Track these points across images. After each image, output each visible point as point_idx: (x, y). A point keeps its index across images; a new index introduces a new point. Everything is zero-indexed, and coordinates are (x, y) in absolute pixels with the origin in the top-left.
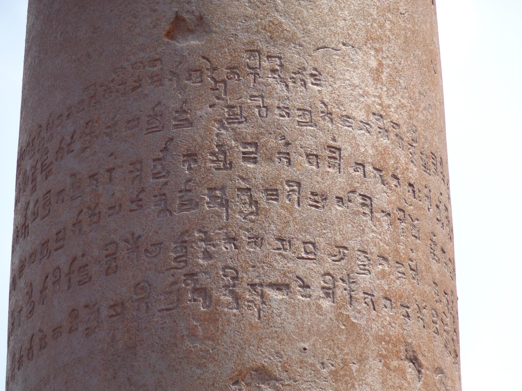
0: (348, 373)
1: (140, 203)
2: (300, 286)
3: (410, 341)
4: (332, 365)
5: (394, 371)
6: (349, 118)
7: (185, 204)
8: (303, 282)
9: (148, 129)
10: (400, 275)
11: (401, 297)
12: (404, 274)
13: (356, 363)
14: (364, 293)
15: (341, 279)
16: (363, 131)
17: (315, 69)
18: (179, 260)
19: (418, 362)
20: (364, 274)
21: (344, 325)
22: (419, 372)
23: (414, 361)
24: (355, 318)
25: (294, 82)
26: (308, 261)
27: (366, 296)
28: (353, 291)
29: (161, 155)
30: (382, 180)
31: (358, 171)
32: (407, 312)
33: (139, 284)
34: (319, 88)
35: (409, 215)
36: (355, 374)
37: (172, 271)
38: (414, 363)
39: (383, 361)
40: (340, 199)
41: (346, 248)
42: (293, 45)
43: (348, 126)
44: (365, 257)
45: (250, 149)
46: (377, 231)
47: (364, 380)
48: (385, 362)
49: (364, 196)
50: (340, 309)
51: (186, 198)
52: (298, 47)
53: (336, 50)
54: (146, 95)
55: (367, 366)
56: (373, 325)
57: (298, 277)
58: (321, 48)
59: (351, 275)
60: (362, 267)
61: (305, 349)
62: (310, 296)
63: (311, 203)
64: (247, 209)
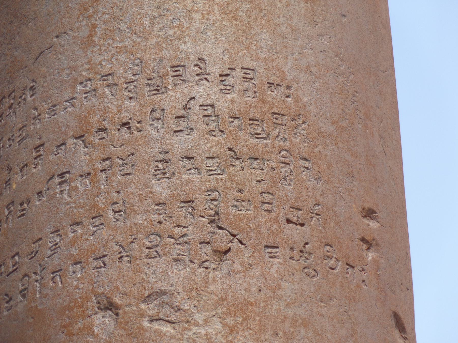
2: (7, 302)
3: (100, 291)
5: (78, 334)
11: (93, 252)
12: (102, 224)
14: (53, 273)
17: (33, 81)
19: (114, 307)
20: (55, 253)
21: (32, 318)
22: (117, 314)
23: (110, 308)
27: (55, 275)
30: (85, 145)
35: (118, 157)
38: (110, 310)
40: (40, 193)
43: (54, 115)
44: (58, 235)
48: (68, 331)
49: (61, 175)
56: (57, 301)
58: (39, 57)
59: (42, 263)
63: (19, 214)
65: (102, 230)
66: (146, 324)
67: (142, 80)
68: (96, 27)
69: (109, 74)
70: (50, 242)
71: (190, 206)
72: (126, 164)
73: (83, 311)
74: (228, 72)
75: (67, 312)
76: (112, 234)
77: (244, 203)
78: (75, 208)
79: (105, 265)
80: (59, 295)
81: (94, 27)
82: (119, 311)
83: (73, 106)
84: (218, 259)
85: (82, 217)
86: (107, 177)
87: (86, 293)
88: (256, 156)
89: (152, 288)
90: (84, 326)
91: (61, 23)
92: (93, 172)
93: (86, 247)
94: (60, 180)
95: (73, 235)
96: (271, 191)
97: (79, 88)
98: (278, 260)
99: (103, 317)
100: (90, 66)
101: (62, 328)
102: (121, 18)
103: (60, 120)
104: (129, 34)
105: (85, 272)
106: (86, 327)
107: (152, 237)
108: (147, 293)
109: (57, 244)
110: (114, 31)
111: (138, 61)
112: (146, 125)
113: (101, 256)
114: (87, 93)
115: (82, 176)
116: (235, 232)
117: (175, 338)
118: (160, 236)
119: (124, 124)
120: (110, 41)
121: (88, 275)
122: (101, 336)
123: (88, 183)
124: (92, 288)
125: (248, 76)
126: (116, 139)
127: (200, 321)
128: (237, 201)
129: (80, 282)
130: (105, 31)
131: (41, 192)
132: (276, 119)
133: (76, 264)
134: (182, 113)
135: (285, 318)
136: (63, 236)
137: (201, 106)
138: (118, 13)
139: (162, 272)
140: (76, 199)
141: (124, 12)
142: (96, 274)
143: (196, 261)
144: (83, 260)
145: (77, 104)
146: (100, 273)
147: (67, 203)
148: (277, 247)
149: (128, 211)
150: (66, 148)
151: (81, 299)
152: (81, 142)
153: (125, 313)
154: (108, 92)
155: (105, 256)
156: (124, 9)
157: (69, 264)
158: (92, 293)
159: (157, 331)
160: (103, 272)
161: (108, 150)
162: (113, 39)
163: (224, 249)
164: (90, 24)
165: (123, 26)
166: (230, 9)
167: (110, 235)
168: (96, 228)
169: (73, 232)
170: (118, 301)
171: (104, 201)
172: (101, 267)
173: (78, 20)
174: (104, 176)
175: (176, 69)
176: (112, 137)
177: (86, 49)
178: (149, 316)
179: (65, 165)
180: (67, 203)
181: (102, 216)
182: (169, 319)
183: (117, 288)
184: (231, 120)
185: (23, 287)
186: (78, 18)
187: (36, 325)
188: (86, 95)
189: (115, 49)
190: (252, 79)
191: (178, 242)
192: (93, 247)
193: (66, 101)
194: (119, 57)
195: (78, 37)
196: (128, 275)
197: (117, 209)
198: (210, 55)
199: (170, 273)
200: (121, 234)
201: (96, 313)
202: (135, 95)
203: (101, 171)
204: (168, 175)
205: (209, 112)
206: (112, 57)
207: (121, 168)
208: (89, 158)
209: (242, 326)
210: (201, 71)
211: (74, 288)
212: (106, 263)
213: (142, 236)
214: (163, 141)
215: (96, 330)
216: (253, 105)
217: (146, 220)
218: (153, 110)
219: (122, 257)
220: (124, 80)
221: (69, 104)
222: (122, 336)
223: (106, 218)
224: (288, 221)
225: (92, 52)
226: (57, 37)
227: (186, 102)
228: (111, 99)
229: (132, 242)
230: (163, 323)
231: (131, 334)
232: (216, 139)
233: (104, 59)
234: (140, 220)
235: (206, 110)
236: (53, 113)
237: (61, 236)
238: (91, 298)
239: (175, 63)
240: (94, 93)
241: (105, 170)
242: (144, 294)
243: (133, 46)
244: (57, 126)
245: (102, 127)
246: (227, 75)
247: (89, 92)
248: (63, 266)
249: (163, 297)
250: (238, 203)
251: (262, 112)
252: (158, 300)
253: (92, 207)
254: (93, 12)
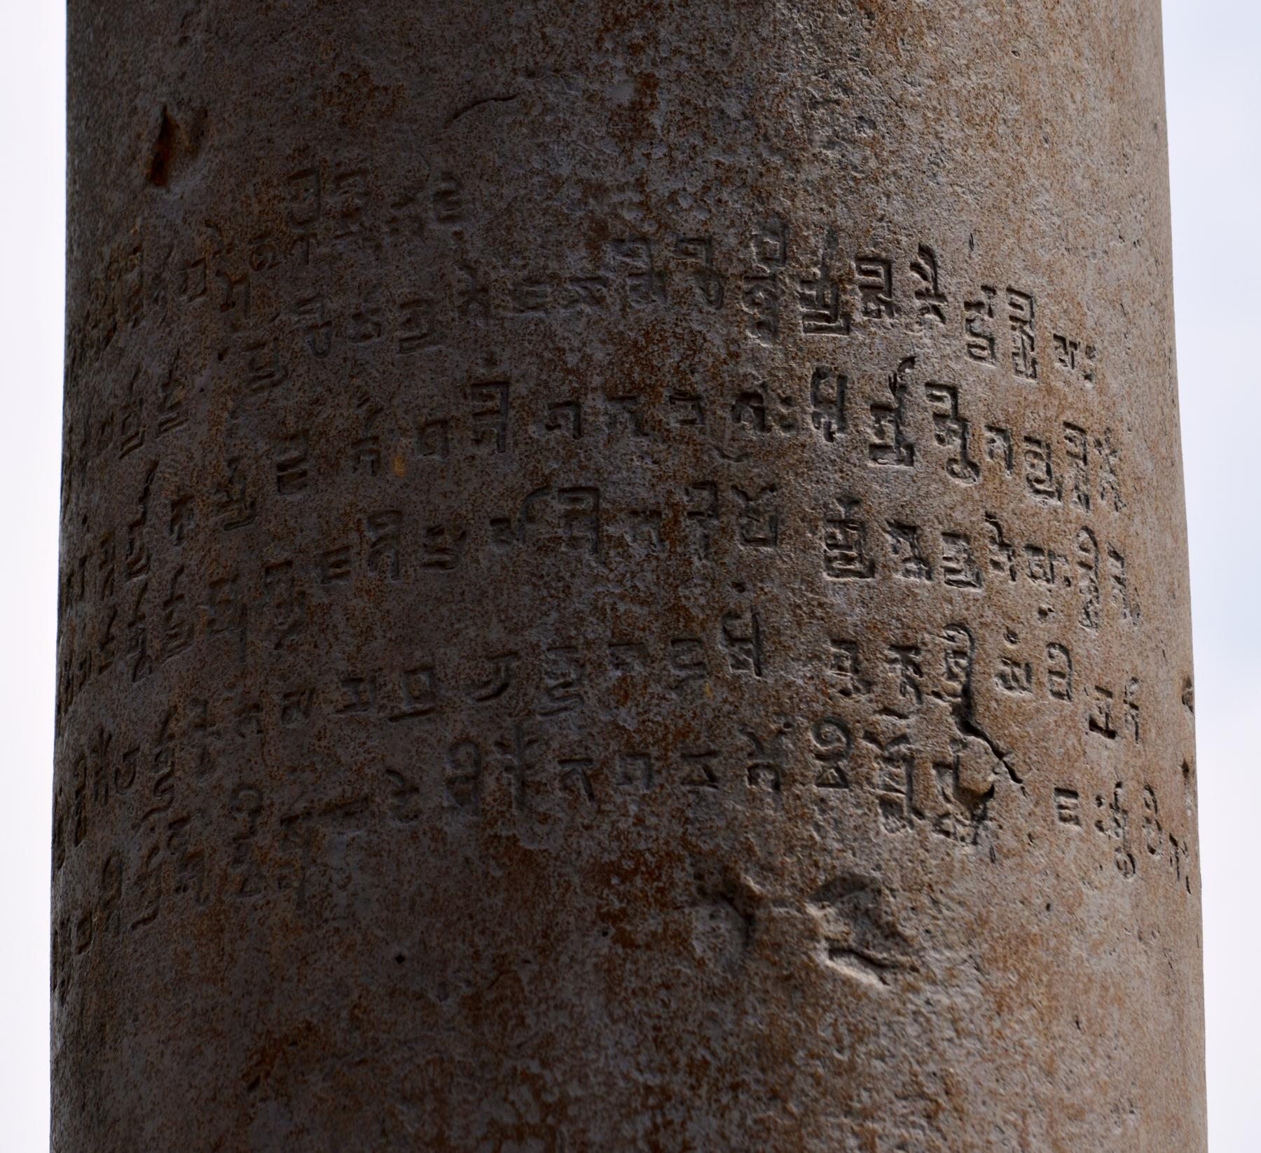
0: (508, 992)
4: (468, 983)
5: (648, 946)
6: (538, 283)
8: (402, 779)
11: (683, 734)
12: (699, 664)
13: (530, 957)
15: (500, 744)
17: (448, 176)
20: (565, 709)
23: (730, 895)
24: (533, 836)
25: (395, 231)
26: (416, 720)
27: (568, 768)
28: (529, 767)
31: (559, 426)
35: (734, 487)
36: (527, 988)
38: (731, 902)
39: (612, 931)
41: (514, 654)
42: (395, 126)
43: (533, 308)
46: (611, 576)
47: (554, 998)
48: (622, 932)
49: (574, 492)
50: (492, 827)
52: (406, 126)
53: (504, 100)
55: (564, 959)
56: (583, 843)
57: (390, 771)
58: (466, 109)
60: (559, 692)
61: (400, 959)
65: (701, 682)
66: (823, 959)
67: (787, 280)
68: (656, 85)
69: (700, 241)
70: (547, 673)
71: (910, 662)
72: (756, 511)
73: (660, 890)
74: (982, 297)
75: (615, 881)
76: (731, 699)
77: (1016, 670)
78: (622, 597)
80: (587, 828)
81: (648, 83)
82: (757, 912)
83: (598, 301)
84: (967, 814)
85: (643, 630)
86: (706, 536)
87: (667, 843)
88: (1038, 542)
89: (834, 867)
90: (665, 930)
91: (544, 34)
92: (668, 513)
93: (659, 718)
95: (619, 673)
96: (1064, 643)
97: (610, 255)
98: (1077, 828)
99: (712, 917)
100: (643, 198)
101: (603, 921)
102: (726, 79)
103: (560, 331)
104: (749, 135)
105: (662, 786)
106: (670, 933)
107: (828, 729)
108: (822, 878)
109: (567, 685)
110: (706, 112)
111: (774, 222)
112: (804, 412)
113: (702, 751)
114: (637, 275)
115: (635, 513)
116: (1001, 745)
117: (888, 1008)
118: (847, 732)
119: (746, 397)
120: (698, 141)
121: (669, 796)
122: (711, 965)
123: (655, 539)
124: (684, 833)
125: (1018, 313)
126: (728, 436)
127: (937, 971)
128: (1006, 664)
129: (648, 809)
130: (681, 104)
131: (506, 520)
132: (1071, 440)
133: (635, 755)
134: (888, 396)
135: (1090, 980)
136: (589, 668)
137: (928, 385)
138: (714, 62)
139: (856, 828)
140: (624, 576)
141: (733, 64)
142: (691, 797)
143: (928, 813)
144: (654, 752)
145: (609, 300)
146: (701, 798)
147: (596, 579)
148: (1074, 794)
149: (768, 646)
150: (577, 416)
151: (653, 855)
152: (627, 415)
153: (772, 919)
154: (698, 291)
155: (712, 754)
156: (733, 55)
157: (615, 752)
158: (685, 848)
159: (847, 982)
160: (711, 799)
161: (706, 458)
162: (704, 137)
163: (984, 788)
164: (636, 70)
165: (733, 109)
166: (982, 112)
167: (725, 701)
168: (683, 674)
169: (617, 666)
170: (752, 884)
171: (702, 601)
172: (702, 783)
173: (600, 48)
174: (699, 532)
175: (871, 267)
176: (716, 427)
177: (628, 145)
178: (827, 939)
179: (582, 468)
180: (596, 579)
181: (699, 641)
182: (872, 953)
183: (750, 850)
184: (989, 434)
186: (599, 41)
187: (517, 890)
188: (636, 282)
189: (712, 169)
190: (1025, 322)
191: (886, 754)
192: (681, 722)
193: (575, 280)
194: (725, 196)
195: (602, 99)
196: (774, 822)
197: (738, 633)
198: (944, 242)
199: (872, 834)
200: (752, 705)
201: (693, 904)
202: (770, 318)
203: (691, 515)
204: (856, 566)
205: (946, 405)
206: (706, 189)
207: (744, 521)
208: (655, 467)
209: (1018, 995)
210: (924, 284)
211: (631, 820)
212: (718, 774)
213: (805, 721)
214: (846, 467)
215: (699, 948)
216: (1031, 398)
217: (812, 678)
218: (819, 375)
219: (756, 766)
220: (741, 268)
221: (582, 292)
222: (766, 978)
223: (710, 652)
224: (1093, 725)
225: (648, 156)
226: (530, 74)
227: (895, 368)
228: (708, 313)
229: (781, 732)
231: (788, 978)
232: (961, 484)
233: (684, 189)
234: (799, 674)
235: (939, 399)
236: (532, 301)
237: (583, 666)
238: (680, 859)
239: (869, 250)
240: (658, 283)
241: (701, 514)
242: (813, 881)
243: (761, 175)
244: (551, 346)
245: (688, 388)
246: (979, 305)
247: (642, 274)
248: (597, 753)
249: (857, 893)
250: (1007, 669)
251: (1047, 419)
252: (845, 899)
253: (670, 610)
254: (644, 38)
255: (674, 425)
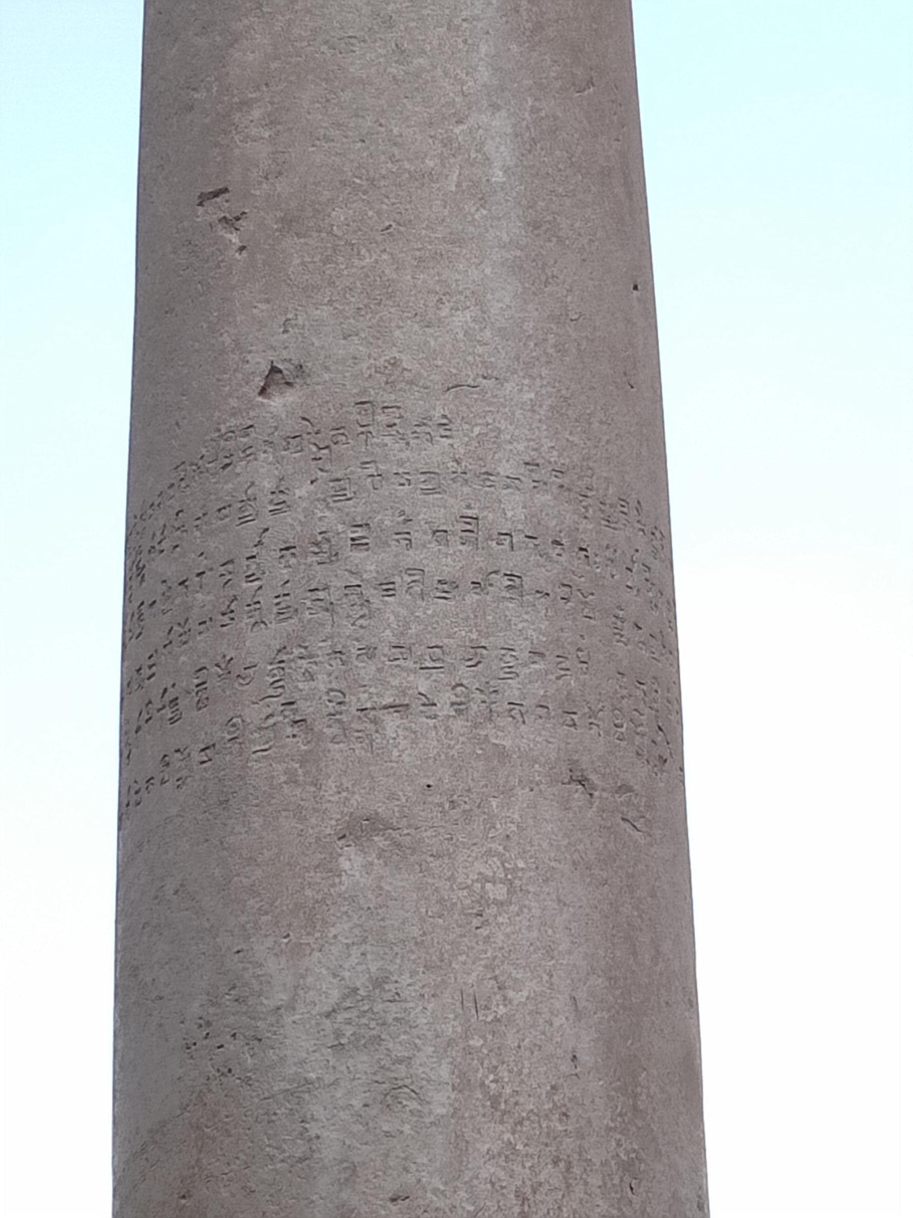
1: (232, 615)
6: (491, 475)
7: (283, 613)
9: (240, 518)
10: (563, 672)
16: (510, 490)
17: (444, 416)
18: (276, 685)
24: (497, 737)
26: (434, 671)
27: (512, 706)
29: (255, 551)
32: (573, 720)
33: (231, 720)
34: (450, 441)
36: (496, 811)
37: (267, 700)
38: (583, 785)
45: (360, 532)
51: (283, 605)
52: (422, 390)
54: (238, 474)
57: (420, 694)
58: (453, 387)
61: (429, 786)
62: (436, 716)
63: (438, 594)
64: (358, 612)
79: (575, 725)
94: (510, 583)
185: (458, 700)
230: (630, 825)
236: (489, 483)
255: (554, 555)
